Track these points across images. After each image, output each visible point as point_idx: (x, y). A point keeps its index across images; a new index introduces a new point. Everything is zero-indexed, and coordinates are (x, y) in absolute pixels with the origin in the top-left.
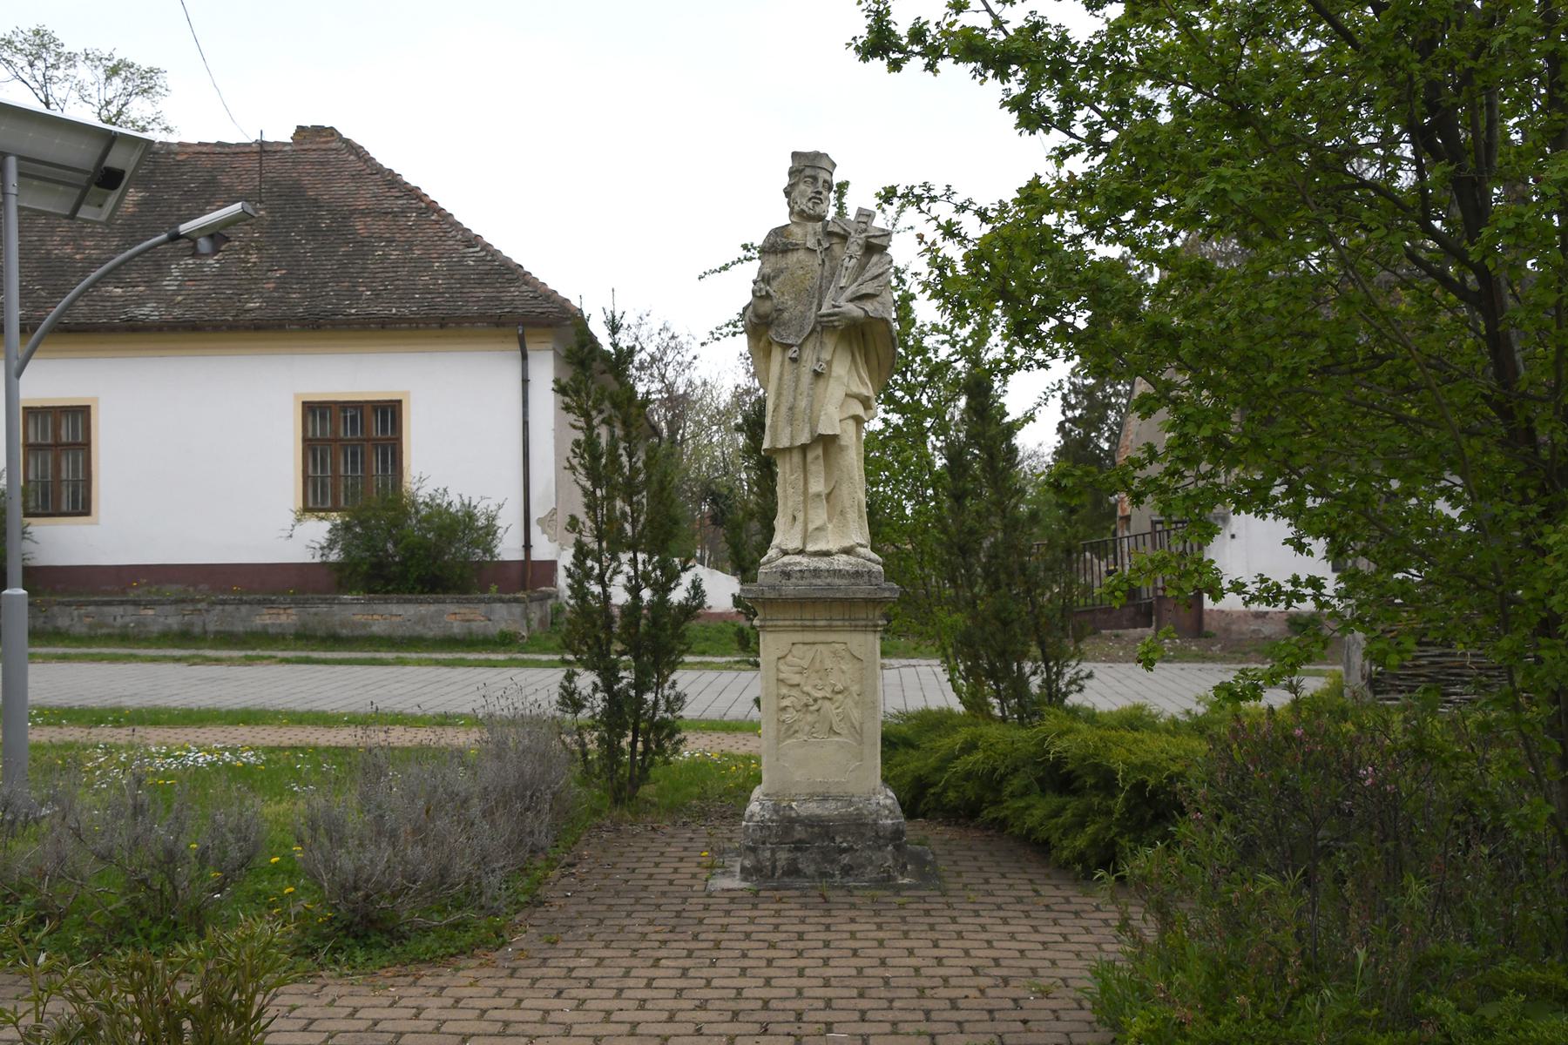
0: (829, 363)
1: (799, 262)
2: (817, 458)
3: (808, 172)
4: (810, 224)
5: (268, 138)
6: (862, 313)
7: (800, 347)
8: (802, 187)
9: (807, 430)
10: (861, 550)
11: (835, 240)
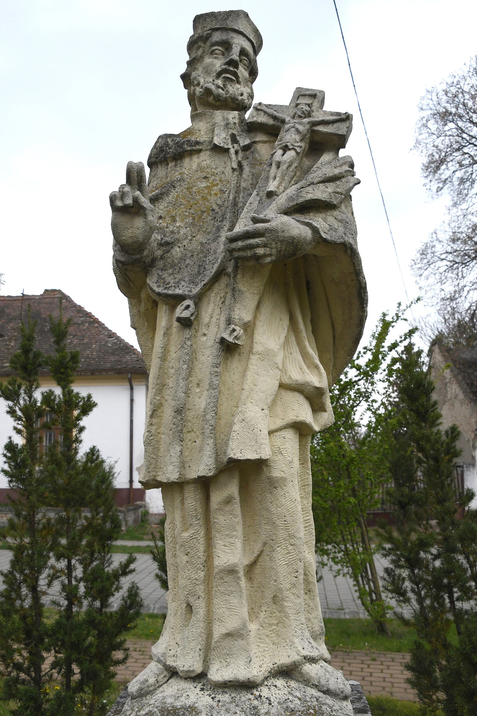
0: (249, 328)
1: (200, 168)
2: (228, 501)
3: (217, 37)
4: (219, 116)
5: (28, 292)
6: (307, 233)
7: (198, 299)
8: (208, 60)
9: (208, 451)
10: (310, 669)
11: (260, 137)
